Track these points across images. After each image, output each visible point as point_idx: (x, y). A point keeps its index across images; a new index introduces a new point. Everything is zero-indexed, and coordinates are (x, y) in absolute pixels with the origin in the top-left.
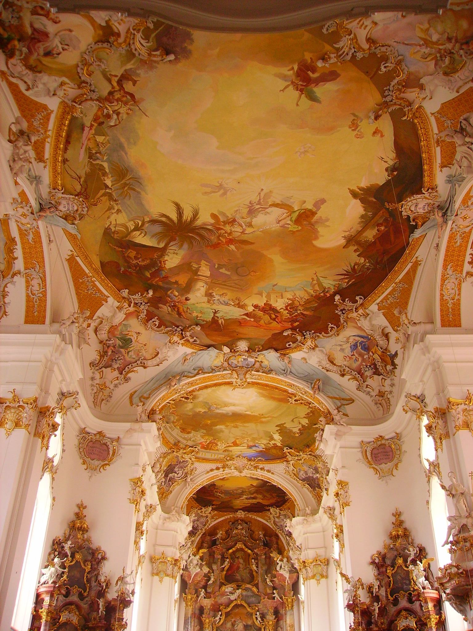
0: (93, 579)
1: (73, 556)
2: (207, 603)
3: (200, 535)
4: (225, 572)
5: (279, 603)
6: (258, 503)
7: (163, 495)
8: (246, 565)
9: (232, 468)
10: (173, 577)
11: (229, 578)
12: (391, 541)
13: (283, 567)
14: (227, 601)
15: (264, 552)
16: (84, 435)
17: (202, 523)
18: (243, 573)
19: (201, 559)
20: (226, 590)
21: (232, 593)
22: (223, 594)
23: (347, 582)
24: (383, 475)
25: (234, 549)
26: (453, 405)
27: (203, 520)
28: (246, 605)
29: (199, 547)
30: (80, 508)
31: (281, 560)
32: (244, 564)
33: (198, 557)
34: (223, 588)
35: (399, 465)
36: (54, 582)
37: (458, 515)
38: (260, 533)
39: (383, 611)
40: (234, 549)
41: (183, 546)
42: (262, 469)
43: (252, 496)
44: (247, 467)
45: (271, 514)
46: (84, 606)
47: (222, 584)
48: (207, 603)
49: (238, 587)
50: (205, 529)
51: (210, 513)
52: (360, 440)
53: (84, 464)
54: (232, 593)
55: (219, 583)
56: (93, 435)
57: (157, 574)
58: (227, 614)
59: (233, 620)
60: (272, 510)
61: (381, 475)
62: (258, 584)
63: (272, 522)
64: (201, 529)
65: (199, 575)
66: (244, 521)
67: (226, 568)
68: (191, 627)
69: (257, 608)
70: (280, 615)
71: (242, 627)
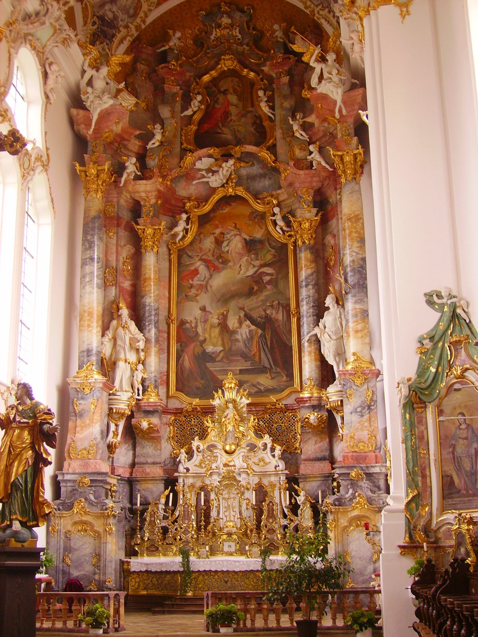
4: (194, 128)
5: (324, 174)
13: (326, 75)
14: (203, 191)
15: (286, 68)
20: (198, 165)
25: (214, 73)
31: (322, 59)
32: (241, 105)
38: (276, 27)
40: (213, 72)
49: (227, 156)
50: (137, 28)
54: (214, 172)
55: (178, 150)
58: (204, 220)
59: (218, 231)
62: (274, 146)
64: (127, 27)
69: (275, 202)
70: (329, 207)
71: (240, 245)
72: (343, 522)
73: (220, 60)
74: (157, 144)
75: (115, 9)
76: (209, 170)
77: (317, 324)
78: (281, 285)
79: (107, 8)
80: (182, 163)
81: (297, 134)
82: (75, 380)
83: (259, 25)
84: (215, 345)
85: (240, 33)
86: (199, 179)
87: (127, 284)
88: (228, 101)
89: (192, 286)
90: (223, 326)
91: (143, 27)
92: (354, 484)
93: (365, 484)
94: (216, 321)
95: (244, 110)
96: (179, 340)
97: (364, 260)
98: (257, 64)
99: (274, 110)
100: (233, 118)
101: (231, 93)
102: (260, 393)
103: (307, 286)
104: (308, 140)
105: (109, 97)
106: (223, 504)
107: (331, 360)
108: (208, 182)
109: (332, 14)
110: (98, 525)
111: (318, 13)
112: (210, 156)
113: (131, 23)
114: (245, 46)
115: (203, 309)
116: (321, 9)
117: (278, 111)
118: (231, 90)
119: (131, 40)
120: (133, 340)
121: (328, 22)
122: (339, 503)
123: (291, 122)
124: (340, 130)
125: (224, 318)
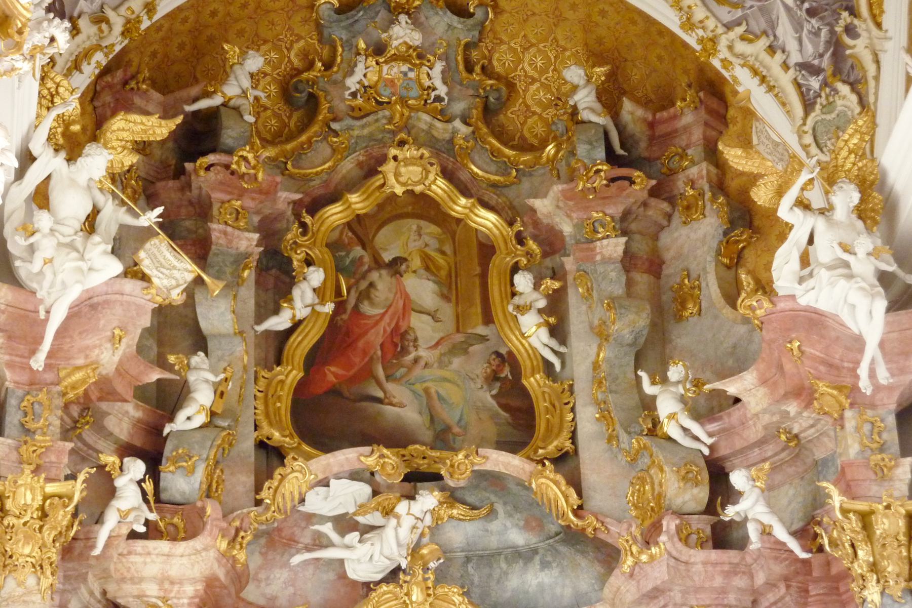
5: (778, 569)
8: (460, 322)
15: (616, 210)
20: (316, 502)
32: (447, 311)
38: (574, 74)
40: (354, 198)
55: (247, 445)
65: (109, 321)
73: (383, 159)
74: (200, 419)
76: (345, 524)
80: (265, 494)
81: (672, 430)
83: (501, 61)
85: (445, 82)
86: (308, 549)
88: (406, 297)
91: (145, 24)
95: (458, 331)
98: (494, 185)
99: (563, 341)
100: (422, 352)
101: (414, 272)
104: (706, 452)
105: (105, 252)
108: (341, 562)
109: (779, 57)
111: (730, 48)
112: (355, 476)
113: (115, 9)
114: (458, 124)
116: (742, 38)
118: (416, 262)
119: (104, 63)
121: (763, 80)
123: (649, 389)
124: (858, 429)
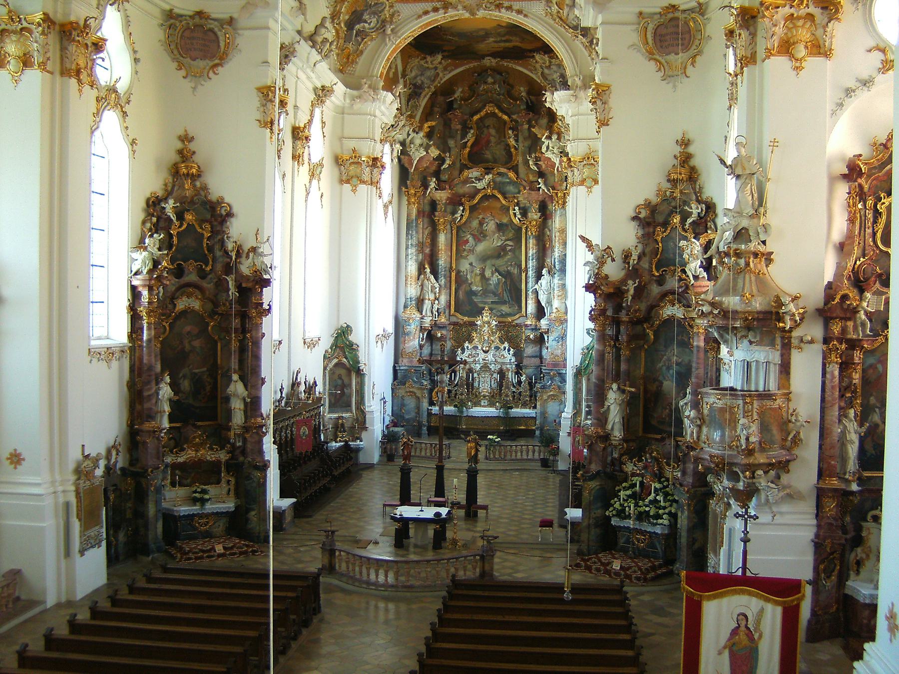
0: (217, 247)
1: (180, 216)
2: (442, 196)
3: (428, 96)
4: (468, 150)
6: (514, 47)
7: (348, 59)
9: (460, 7)
10: (372, 183)
11: (476, 158)
12: (669, 185)
14: (472, 190)
16: (172, 21)
17: (429, 78)
18: (494, 151)
19: (429, 136)
21: (479, 179)
22: (467, 181)
23: (589, 251)
24: (670, 73)
26: (767, 9)
27: (429, 73)
28: (499, 196)
29: (428, 115)
30: (183, 141)
31: (549, 138)
33: (421, 134)
34: (466, 173)
35: (698, 58)
36: (150, 272)
37: (738, 210)
38: (522, 89)
39: (640, 291)
41: (392, 126)
42: (509, 8)
43: (503, 39)
44: (484, 5)
45: (536, 62)
46: (208, 285)
47: (464, 167)
48: (442, 196)
49: (488, 170)
51: (440, 63)
52: (637, 10)
53: (181, 69)
56: (188, 18)
57: (348, 182)
59: (481, 217)
60: (538, 57)
61: (669, 74)
62: (517, 165)
63: (540, 74)
64: (429, 87)
66: (497, 71)
67: (469, 144)
68: (417, 232)
69: (516, 201)
70: (548, 212)
71: (494, 227)
72: (545, 397)
73: (485, 106)
75: (423, 78)
76: (477, 179)
77: (537, 283)
78: (517, 253)
79: (418, 78)
82: (403, 316)
83: (511, 82)
84: (477, 286)
87: (427, 251)
89: (464, 250)
90: (482, 275)
92: (552, 379)
93: (557, 379)
94: (478, 272)
96: (456, 282)
97: (565, 255)
102: (502, 316)
103: (532, 260)
106: (482, 379)
107: (543, 304)
110: (419, 394)
115: (471, 264)
117: (521, 145)
120: (433, 288)
122: (544, 387)
125: (483, 270)
